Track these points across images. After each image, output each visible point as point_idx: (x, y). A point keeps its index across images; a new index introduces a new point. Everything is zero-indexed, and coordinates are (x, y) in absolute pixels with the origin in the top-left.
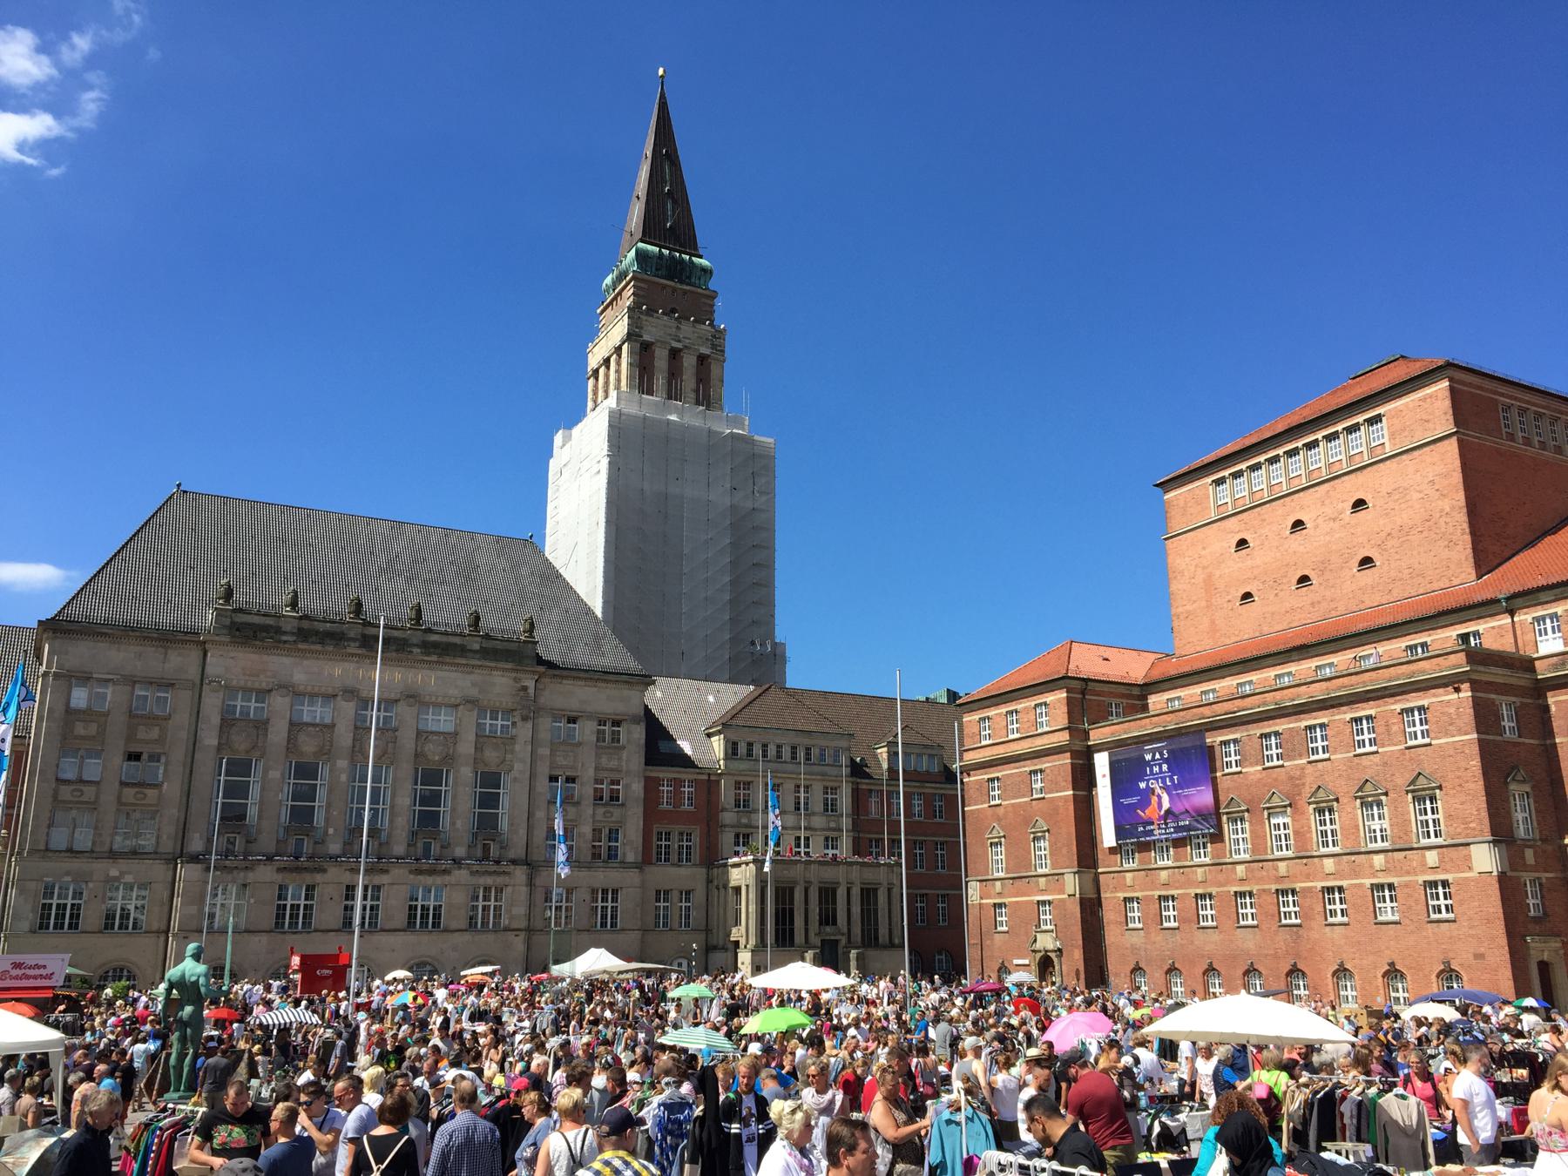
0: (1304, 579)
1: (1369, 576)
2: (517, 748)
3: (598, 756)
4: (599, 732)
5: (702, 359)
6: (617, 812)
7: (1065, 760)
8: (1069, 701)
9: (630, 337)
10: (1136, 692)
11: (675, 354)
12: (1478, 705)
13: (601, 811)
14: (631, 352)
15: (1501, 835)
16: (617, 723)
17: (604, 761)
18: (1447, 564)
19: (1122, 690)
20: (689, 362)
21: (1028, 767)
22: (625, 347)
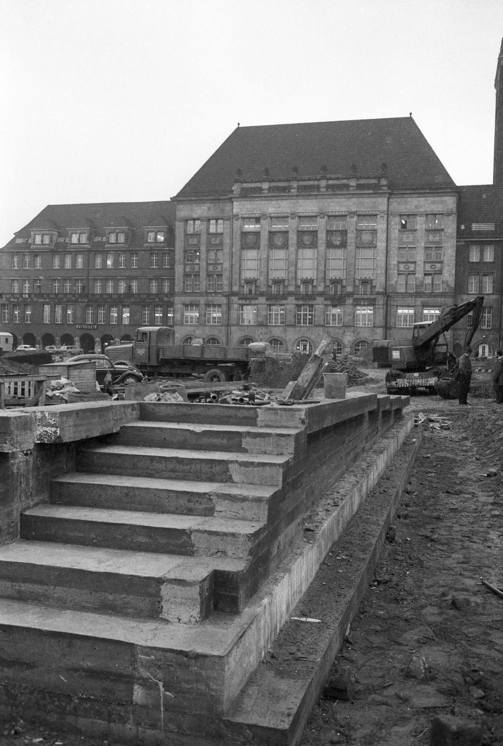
2: (378, 235)
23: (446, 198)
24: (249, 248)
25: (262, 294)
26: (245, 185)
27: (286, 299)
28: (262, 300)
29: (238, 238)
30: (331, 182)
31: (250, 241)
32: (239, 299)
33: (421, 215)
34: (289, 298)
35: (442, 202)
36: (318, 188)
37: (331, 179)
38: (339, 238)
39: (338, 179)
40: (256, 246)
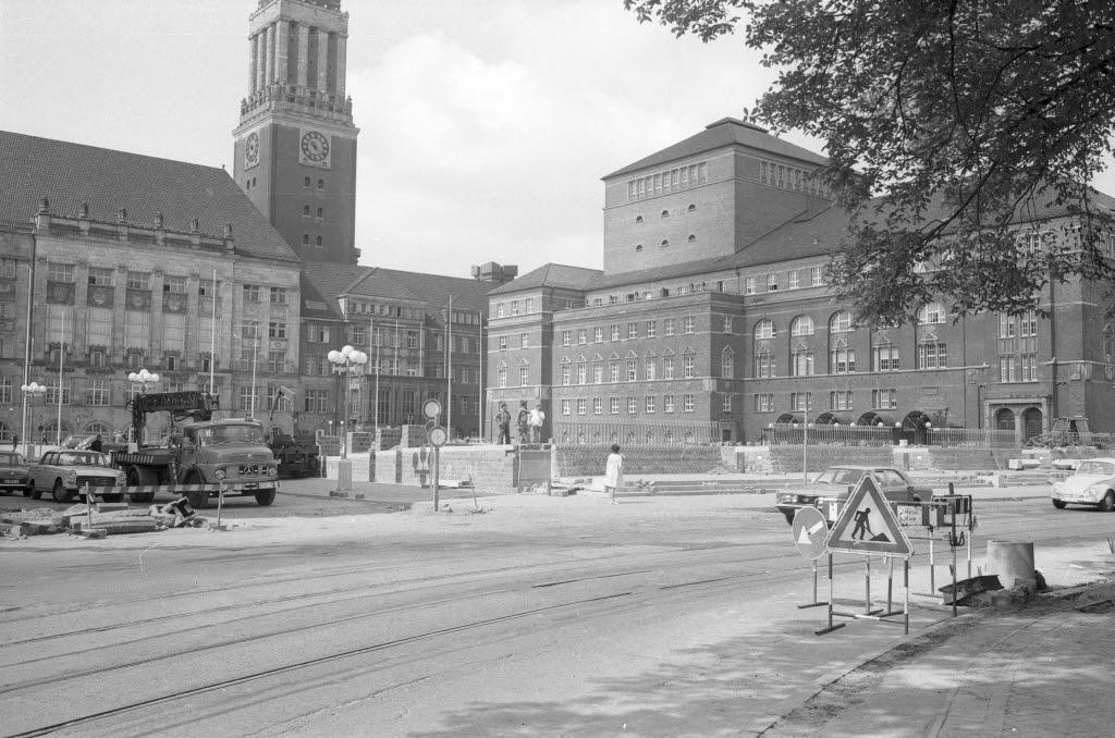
0: (665, 242)
1: (692, 246)
3: (272, 310)
4: (272, 296)
5: (332, 35)
6: (283, 344)
7: (539, 329)
8: (544, 299)
9: (282, 18)
10: (580, 294)
11: (313, 30)
12: (713, 318)
13: (273, 343)
14: (282, 29)
15: (715, 372)
16: (283, 290)
17: (275, 312)
18: (725, 247)
19: (574, 293)
20: (323, 37)
21: (520, 331)
22: (278, 24)
23: (291, 272)
24: (56, 302)
25: (79, 365)
26: (55, 221)
27: (114, 372)
28: (81, 372)
29: (44, 286)
30: (169, 235)
31: (59, 291)
32: (48, 369)
33: (266, 287)
34: (118, 372)
35: (287, 276)
36: (154, 240)
37: (169, 231)
38: (178, 303)
39: (178, 233)
40: (68, 300)
